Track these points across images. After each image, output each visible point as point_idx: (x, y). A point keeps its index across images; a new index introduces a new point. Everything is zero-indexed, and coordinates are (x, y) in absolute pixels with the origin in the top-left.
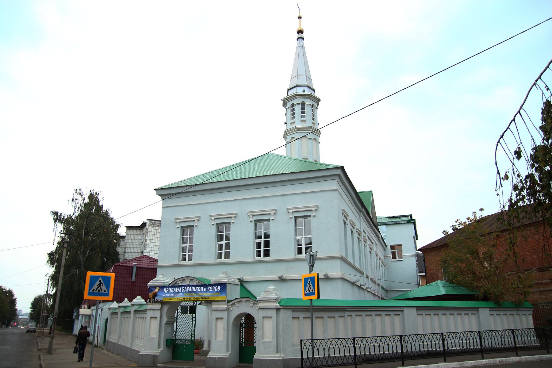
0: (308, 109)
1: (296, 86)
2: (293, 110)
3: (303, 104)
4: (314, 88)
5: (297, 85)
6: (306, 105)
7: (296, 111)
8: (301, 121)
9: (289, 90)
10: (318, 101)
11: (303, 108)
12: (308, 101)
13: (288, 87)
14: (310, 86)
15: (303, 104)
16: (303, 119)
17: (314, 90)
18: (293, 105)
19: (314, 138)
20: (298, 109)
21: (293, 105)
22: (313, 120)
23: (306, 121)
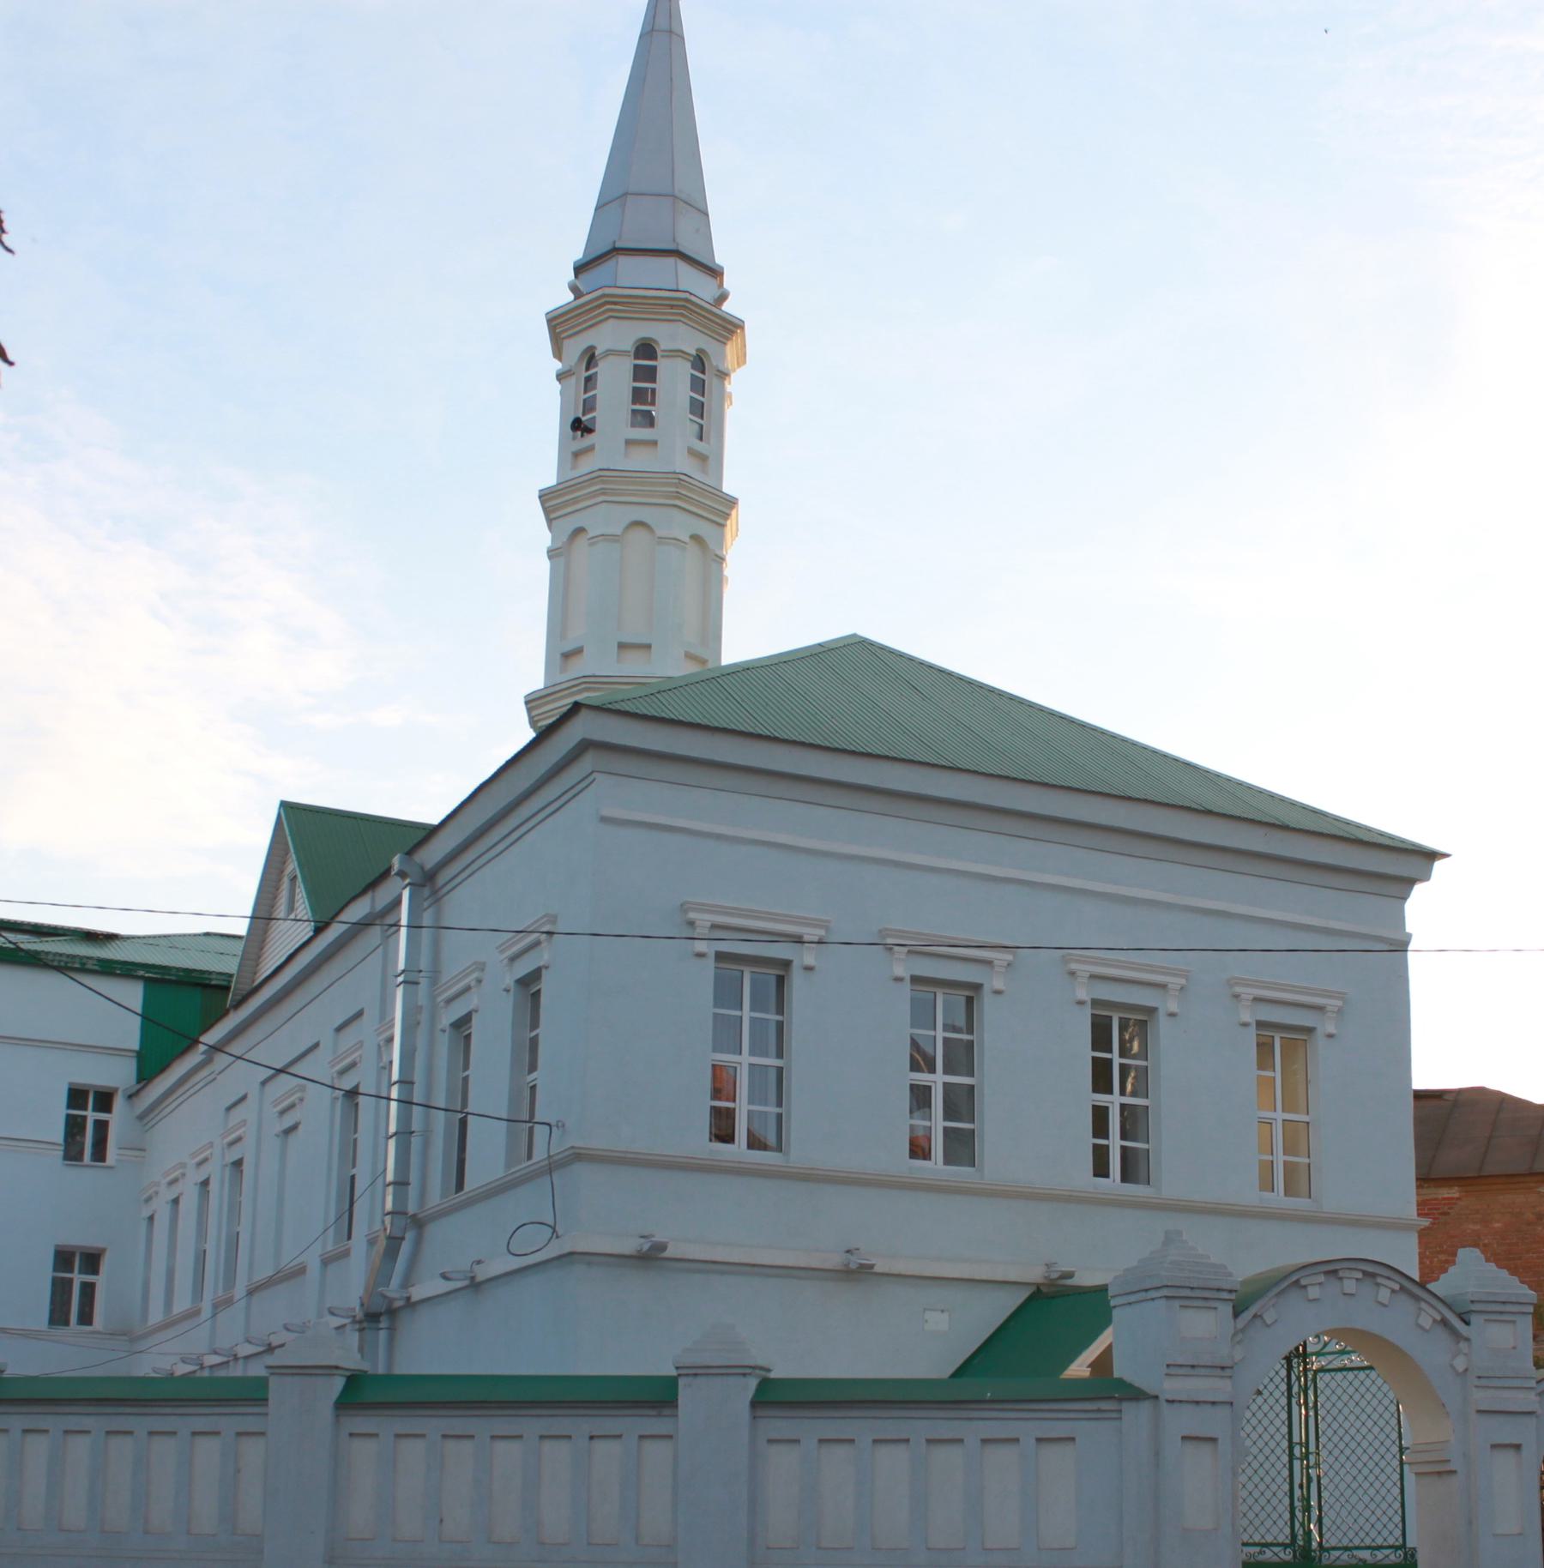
0: (673, 379)
1: (615, 251)
2: (590, 382)
3: (646, 349)
4: (720, 258)
5: (618, 245)
6: (659, 354)
7: (601, 391)
8: (629, 443)
9: (579, 269)
10: (731, 328)
11: (648, 374)
12: (673, 336)
13: (578, 253)
14: (686, 247)
15: (646, 349)
16: (643, 433)
17: (715, 273)
18: (590, 358)
19: (696, 538)
20: (616, 379)
21: (590, 358)
22: (701, 439)
23: (654, 443)
